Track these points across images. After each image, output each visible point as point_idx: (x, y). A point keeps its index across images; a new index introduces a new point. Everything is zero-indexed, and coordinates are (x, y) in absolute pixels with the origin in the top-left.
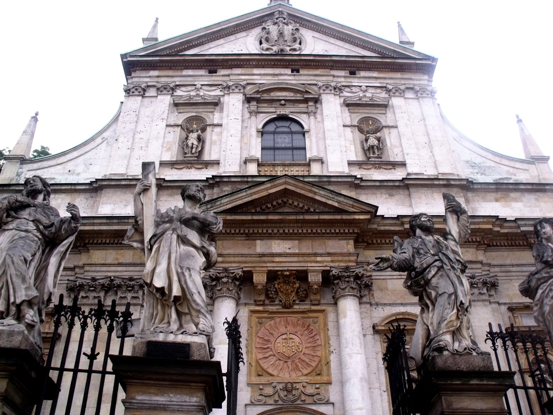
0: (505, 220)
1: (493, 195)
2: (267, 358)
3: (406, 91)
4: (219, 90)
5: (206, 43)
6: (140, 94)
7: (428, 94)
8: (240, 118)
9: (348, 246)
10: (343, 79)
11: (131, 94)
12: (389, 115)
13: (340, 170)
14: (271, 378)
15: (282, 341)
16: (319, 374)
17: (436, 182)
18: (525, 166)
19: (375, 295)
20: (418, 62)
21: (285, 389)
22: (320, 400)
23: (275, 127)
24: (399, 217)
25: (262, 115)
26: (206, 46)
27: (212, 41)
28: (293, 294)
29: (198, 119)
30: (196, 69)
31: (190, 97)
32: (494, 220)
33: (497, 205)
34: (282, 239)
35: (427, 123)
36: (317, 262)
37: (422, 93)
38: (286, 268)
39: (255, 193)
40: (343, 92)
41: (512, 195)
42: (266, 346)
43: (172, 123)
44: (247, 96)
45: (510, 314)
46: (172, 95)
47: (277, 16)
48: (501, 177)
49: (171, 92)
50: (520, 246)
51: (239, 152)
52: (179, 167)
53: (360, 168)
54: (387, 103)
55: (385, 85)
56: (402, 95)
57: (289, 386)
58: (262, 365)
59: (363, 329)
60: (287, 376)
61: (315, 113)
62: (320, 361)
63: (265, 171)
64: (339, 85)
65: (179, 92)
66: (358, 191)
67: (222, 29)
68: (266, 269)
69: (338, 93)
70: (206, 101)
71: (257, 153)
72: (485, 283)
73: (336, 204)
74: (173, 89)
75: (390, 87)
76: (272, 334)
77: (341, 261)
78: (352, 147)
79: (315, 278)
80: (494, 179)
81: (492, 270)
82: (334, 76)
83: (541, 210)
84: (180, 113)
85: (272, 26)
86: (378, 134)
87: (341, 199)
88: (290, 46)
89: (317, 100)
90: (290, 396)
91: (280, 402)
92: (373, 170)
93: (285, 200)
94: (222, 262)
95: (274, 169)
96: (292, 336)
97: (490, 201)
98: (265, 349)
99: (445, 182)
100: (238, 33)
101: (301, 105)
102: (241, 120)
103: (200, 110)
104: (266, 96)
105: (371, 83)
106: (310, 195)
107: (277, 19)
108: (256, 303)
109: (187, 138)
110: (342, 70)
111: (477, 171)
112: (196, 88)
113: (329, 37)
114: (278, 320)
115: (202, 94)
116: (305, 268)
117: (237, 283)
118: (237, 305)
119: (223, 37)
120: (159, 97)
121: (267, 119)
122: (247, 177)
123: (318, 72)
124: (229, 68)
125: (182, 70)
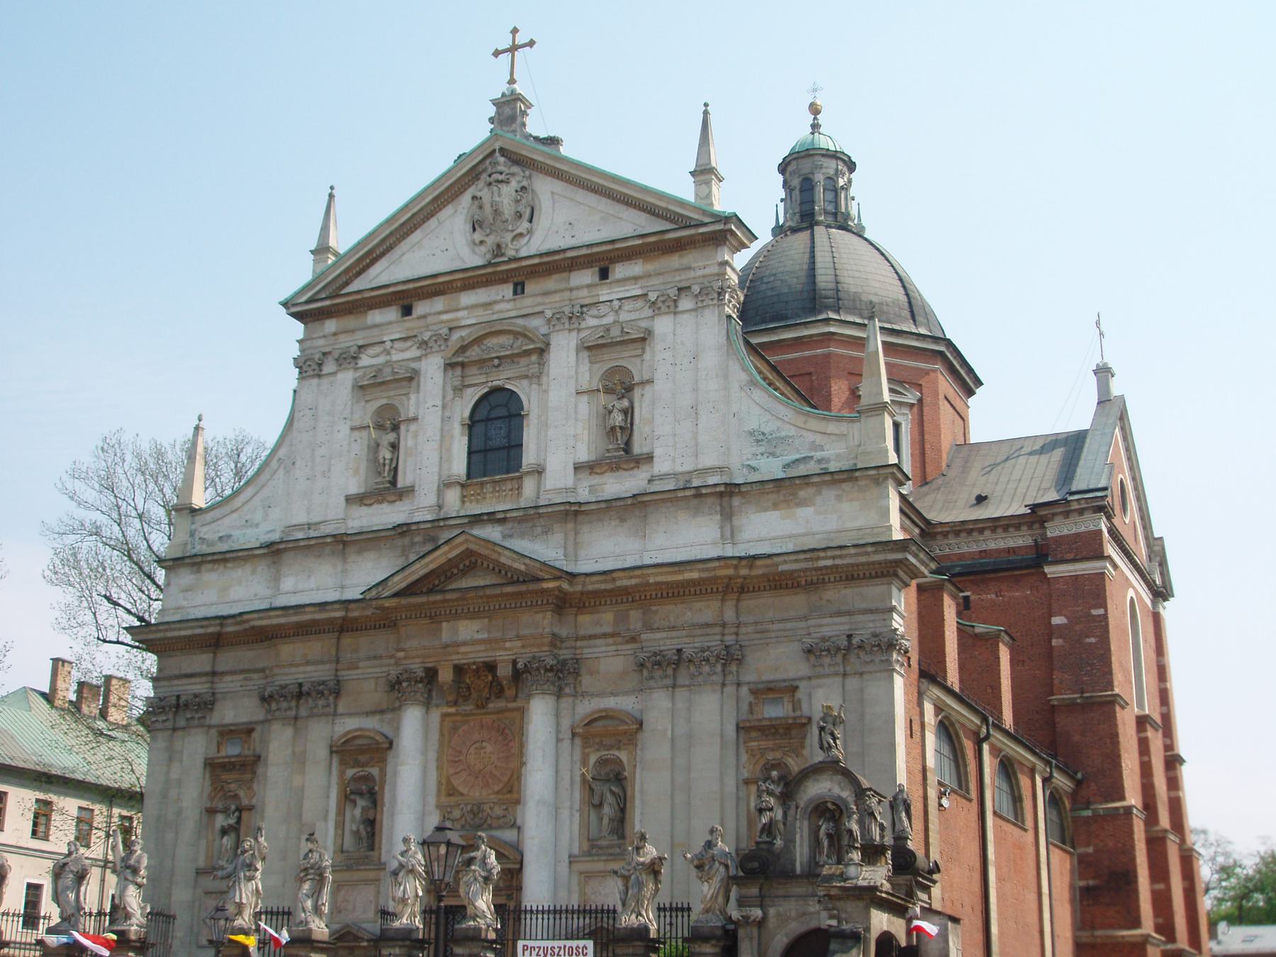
1: (773, 497)
2: (456, 773)
3: (683, 295)
4: (415, 347)
5: (396, 245)
6: (316, 372)
7: (712, 299)
8: (439, 403)
9: (544, 622)
10: (585, 292)
11: (304, 375)
12: (647, 356)
13: (560, 484)
14: (460, 798)
16: (510, 792)
17: (680, 494)
18: (842, 428)
19: (584, 681)
20: (701, 230)
21: (472, 811)
22: (505, 824)
23: (489, 408)
24: (604, 573)
25: (470, 391)
26: (397, 251)
27: (404, 239)
28: (487, 690)
29: (389, 408)
30: (384, 307)
31: (379, 370)
32: (735, 562)
33: (773, 515)
34: (471, 619)
35: (700, 366)
36: (506, 649)
37: (705, 297)
39: (431, 562)
40: (587, 317)
41: (802, 494)
43: (357, 424)
44: (448, 362)
45: (751, 699)
46: (356, 369)
47: (489, 171)
48: (798, 456)
49: (353, 362)
50: (787, 587)
51: (436, 469)
52: (368, 502)
53: (591, 474)
54: (642, 335)
55: (645, 292)
56: (672, 309)
57: (475, 808)
59: (558, 731)
60: (477, 794)
61: (539, 377)
62: (512, 775)
63: (473, 495)
64: (577, 308)
65: (365, 360)
66: (580, 518)
67: (413, 215)
69: (576, 326)
70: (397, 377)
71: (459, 466)
72: (718, 657)
73: (523, 568)
74: (355, 358)
75: (653, 296)
78: (586, 432)
79: (504, 671)
80: (785, 463)
81: (743, 630)
82: (571, 290)
84: (367, 401)
85: (486, 189)
86: (625, 403)
87: (527, 561)
88: (513, 231)
89: (542, 351)
90: (477, 820)
91: (467, 826)
92: (608, 474)
93: (473, 559)
94: (405, 658)
95: (482, 489)
96: (484, 744)
97: (766, 510)
98: (456, 762)
100: (440, 210)
101: (524, 361)
102: (440, 408)
103: (392, 393)
104: (474, 353)
105: (628, 290)
106: (495, 556)
107: (490, 176)
108: (448, 704)
109: (378, 445)
110: (587, 268)
111: (762, 449)
112: (385, 350)
113: (576, 189)
114: (472, 724)
115: (396, 357)
116: (493, 659)
117: (420, 685)
118: (428, 709)
119: (420, 225)
120: (340, 376)
121: (476, 398)
122: (438, 520)
123: (551, 283)
124: (427, 298)
125: (365, 312)
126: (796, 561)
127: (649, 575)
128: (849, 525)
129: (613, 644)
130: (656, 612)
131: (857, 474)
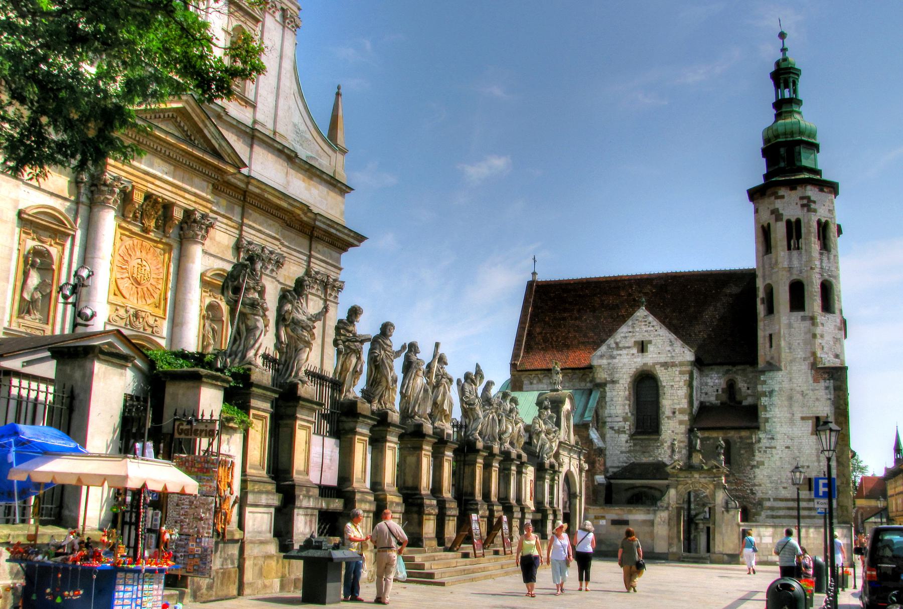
0: (311, 211)
15: (137, 266)
34: (162, 160)
38: (160, 195)
42: (124, 267)
58: (119, 285)
68: (145, 188)
73: (217, 146)
76: (130, 255)
77: (201, 205)
79: (178, 214)
83: (327, 204)
87: (224, 144)
91: (129, 327)
93: (175, 116)
94: (114, 166)
96: (144, 263)
99: (281, 148)
106: (201, 125)
114: (136, 241)
116: (174, 201)
126: (324, 223)
127: (266, 191)
128: (330, 211)
129: (227, 225)
130: (251, 214)
131: (339, 185)
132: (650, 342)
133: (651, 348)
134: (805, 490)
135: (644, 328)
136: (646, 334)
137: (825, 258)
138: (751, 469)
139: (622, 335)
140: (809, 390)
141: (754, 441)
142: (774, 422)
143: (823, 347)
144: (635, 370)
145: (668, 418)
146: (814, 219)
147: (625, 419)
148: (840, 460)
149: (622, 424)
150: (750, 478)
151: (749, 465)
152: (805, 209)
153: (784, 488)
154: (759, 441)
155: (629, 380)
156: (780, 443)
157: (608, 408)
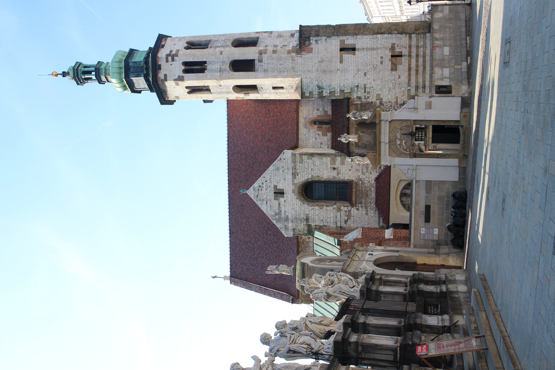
132: (275, 187)
133: (280, 187)
134: (402, 59)
135: (264, 190)
136: (268, 190)
137: (216, 44)
138: (383, 105)
139: (269, 210)
140: (318, 57)
141: (360, 102)
142: (344, 85)
143: (284, 46)
144: (298, 200)
145: (338, 174)
146: (183, 52)
147: (339, 210)
148: (376, 31)
149: (342, 213)
150: (391, 106)
151: (379, 107)
152: (175, 58)
153: (399, 78)
154: (360, 98)
155: (306, 206)
156: (361, 80)
157: (329, 224)
